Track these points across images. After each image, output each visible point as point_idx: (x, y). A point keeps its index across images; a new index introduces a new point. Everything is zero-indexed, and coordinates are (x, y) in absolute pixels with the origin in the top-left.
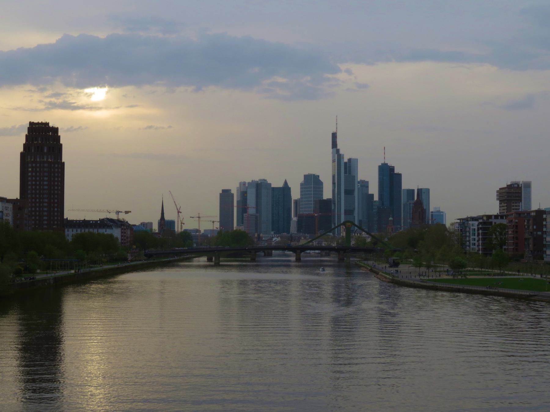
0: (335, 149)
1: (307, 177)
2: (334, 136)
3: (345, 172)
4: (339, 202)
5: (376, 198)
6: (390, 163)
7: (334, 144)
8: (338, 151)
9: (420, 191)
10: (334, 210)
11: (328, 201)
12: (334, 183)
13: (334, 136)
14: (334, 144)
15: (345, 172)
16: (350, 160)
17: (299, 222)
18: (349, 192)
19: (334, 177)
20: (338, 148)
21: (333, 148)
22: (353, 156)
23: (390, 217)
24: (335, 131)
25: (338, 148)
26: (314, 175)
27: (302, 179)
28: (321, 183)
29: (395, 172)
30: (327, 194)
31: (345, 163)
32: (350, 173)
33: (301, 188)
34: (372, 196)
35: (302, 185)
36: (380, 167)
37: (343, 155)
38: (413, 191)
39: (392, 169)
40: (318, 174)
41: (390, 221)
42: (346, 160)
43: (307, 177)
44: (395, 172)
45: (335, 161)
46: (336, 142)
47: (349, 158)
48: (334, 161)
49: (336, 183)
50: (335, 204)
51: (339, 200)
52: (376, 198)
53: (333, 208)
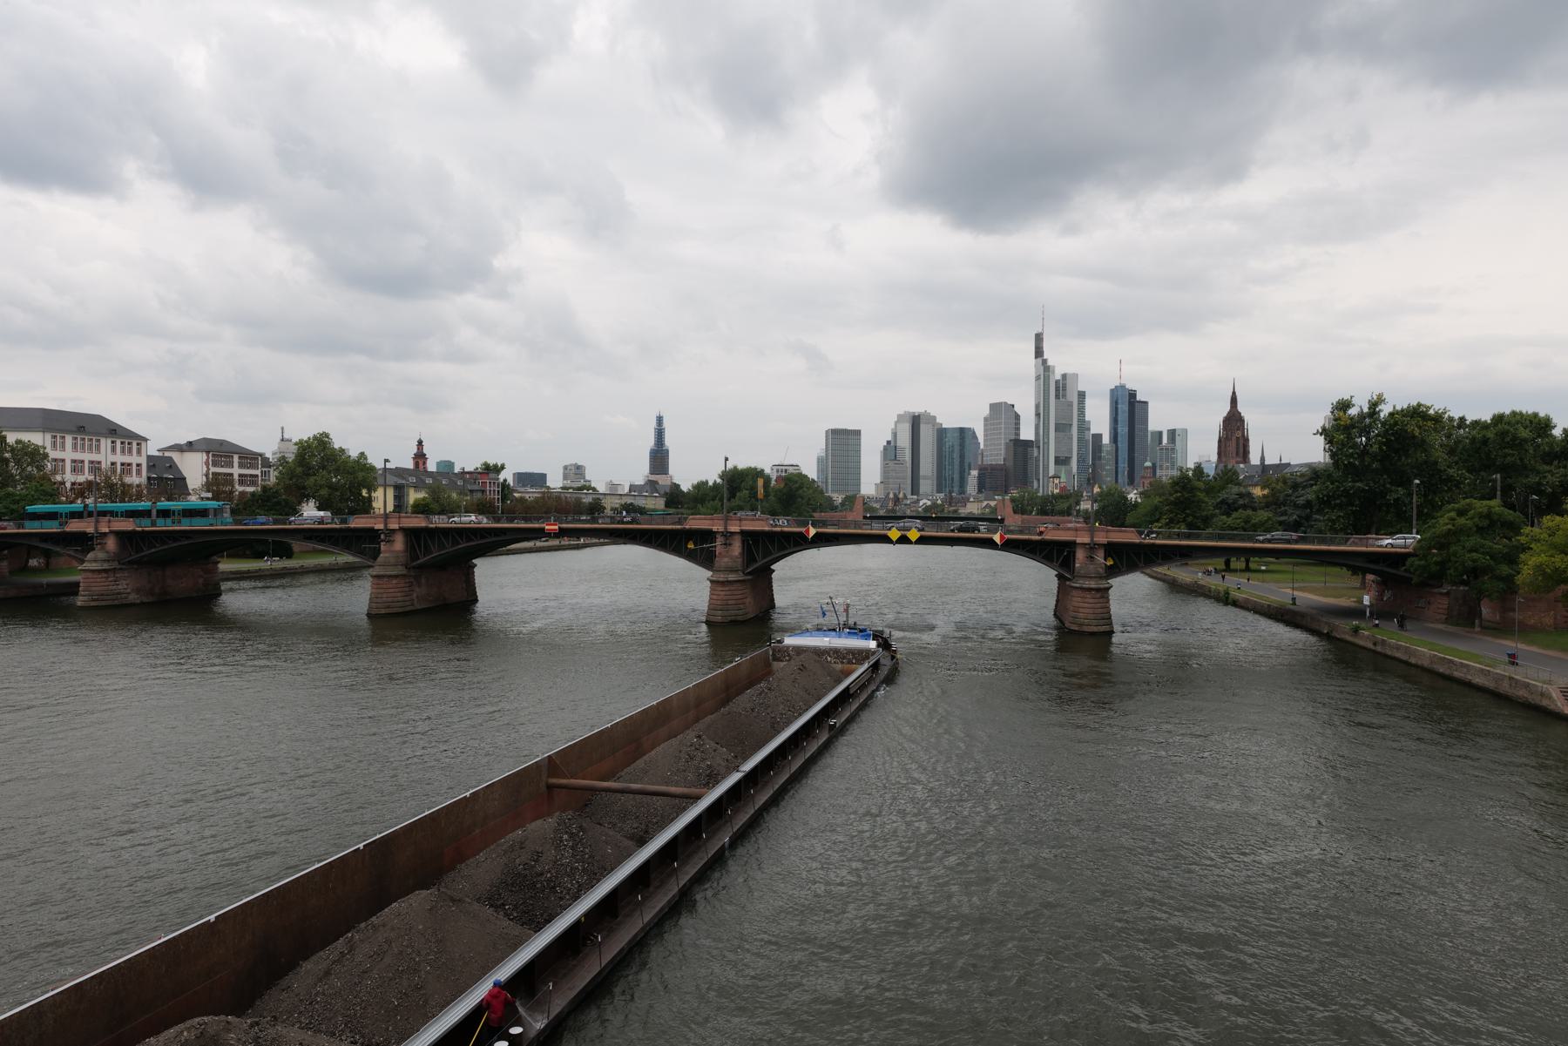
0: (1040, 360)
1: (996, 408)
2: (1039, 338)
3: (1056, 396)
4: (1047, 443)
5: (1106, 440)
6: (1130, 386)
7: (1039, 352)
8: (1045, 362)
9: (1172, 434)
10: (1037, 460)
11: (1028, 443)
12: (1038, 415)
13: (1039, 338)
14: (1039, 352)
15: (1057, 397)
16: (1064, 376)
17: (981, 478)
18: (1062, 428)
19: (1037, 406)
20: (1045, 357)
21: (1036, 357)
22: (1069, 370)
23: (1146, 461)
24: (1040, 331)
25: (1045, 357)
26: (1006, 403)
27: (986, 412)
28: (1017, 417)
29: (1138, 399)
30: (1027, 433)
31: (1057, 382)
32: (1064, 396)
33: (985, 425)
34: (1098, 437)
35: (986, 419)
36: (1112, 391)
37: (1054, 367)
38: (1160, 433)
39: (1132, 395)
40: (1012, 403)
41: (1147, 468)
42: (1058, 377)
43: (996, 408)
44: (1138, 399)
45: (1040, 379)
46: (1042, 348)
47: (1063, 373)
48: (1038, 378)
49: (1041, 414)
50: (1039, 447)
51: (1046, 440)
52: (1106, 440)
53: (1035, 454)
